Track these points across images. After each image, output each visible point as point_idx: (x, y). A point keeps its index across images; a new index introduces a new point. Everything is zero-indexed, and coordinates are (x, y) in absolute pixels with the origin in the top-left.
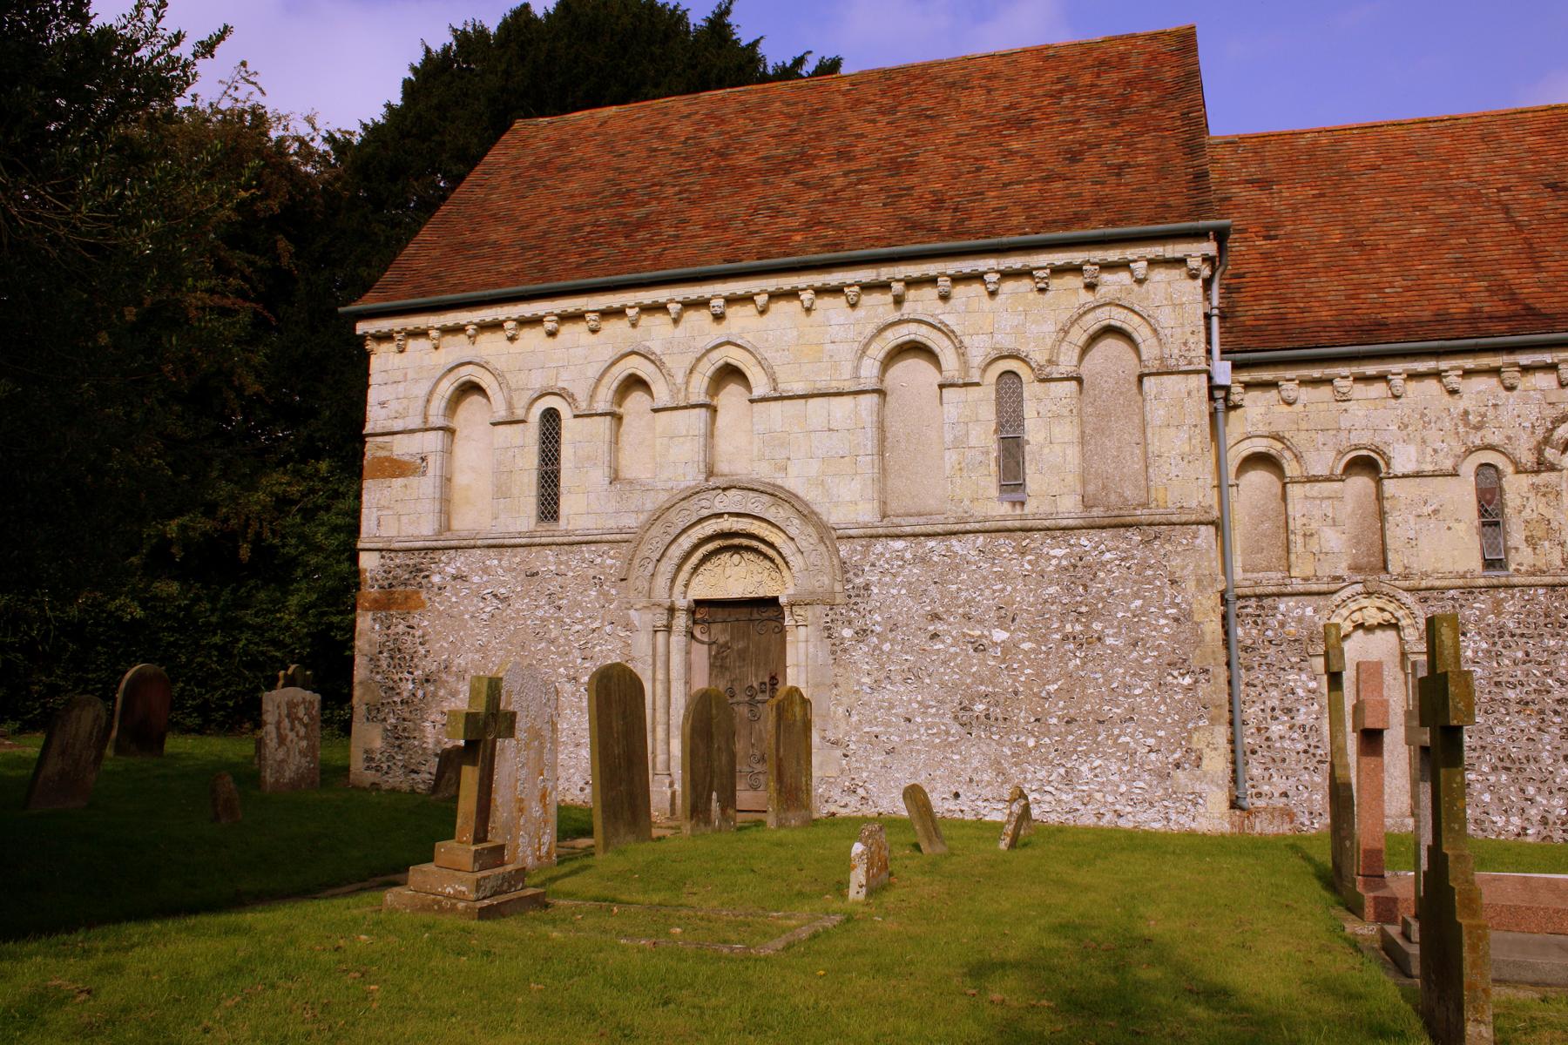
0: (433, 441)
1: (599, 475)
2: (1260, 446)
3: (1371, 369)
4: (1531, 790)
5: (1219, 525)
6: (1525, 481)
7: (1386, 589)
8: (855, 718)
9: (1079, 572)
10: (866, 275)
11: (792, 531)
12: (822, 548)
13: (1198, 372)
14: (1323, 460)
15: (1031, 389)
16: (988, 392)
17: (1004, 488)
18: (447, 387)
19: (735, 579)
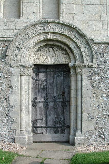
8: (100, 109)
11: (75, 40)
12: (87, 46)
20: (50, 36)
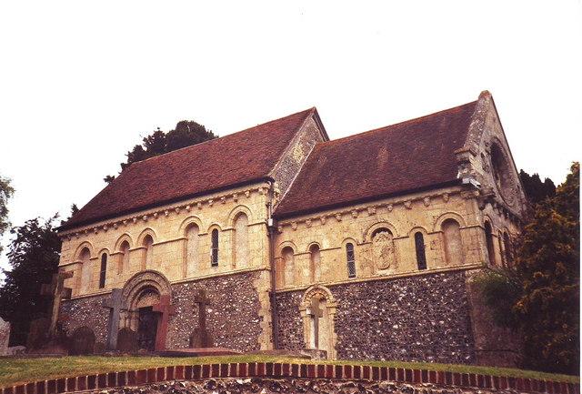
0: (76, 267)
1: (115, 272)
2: (287, 244)
3: (315, 216)
4: (365, 353)
5: (271, 271)
6: (361, 247)
7: (321, 287)
9: (230, 289)
10: (179, 205)
13: (262, 223)
14: (303, 248)
15: (220, 234)
16: (210, 236)
17: (213, 265)
18: (80, 249)
19: (149, 301)
20: (145, 284)
